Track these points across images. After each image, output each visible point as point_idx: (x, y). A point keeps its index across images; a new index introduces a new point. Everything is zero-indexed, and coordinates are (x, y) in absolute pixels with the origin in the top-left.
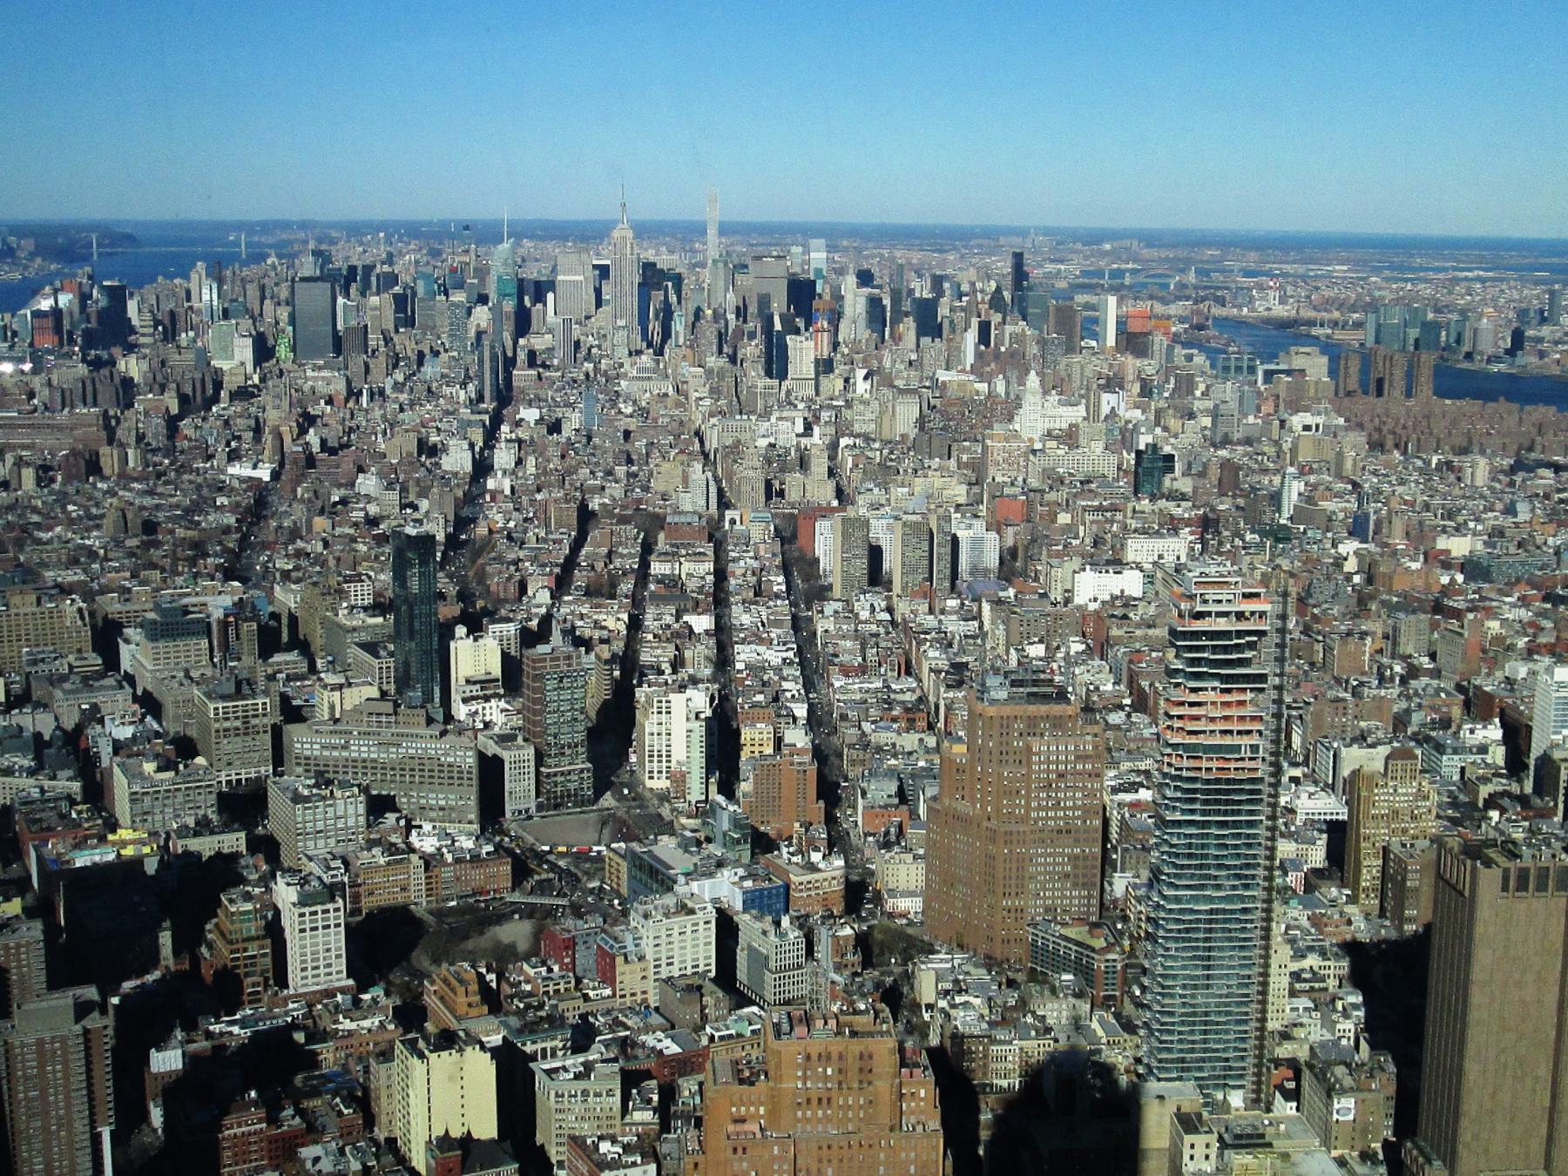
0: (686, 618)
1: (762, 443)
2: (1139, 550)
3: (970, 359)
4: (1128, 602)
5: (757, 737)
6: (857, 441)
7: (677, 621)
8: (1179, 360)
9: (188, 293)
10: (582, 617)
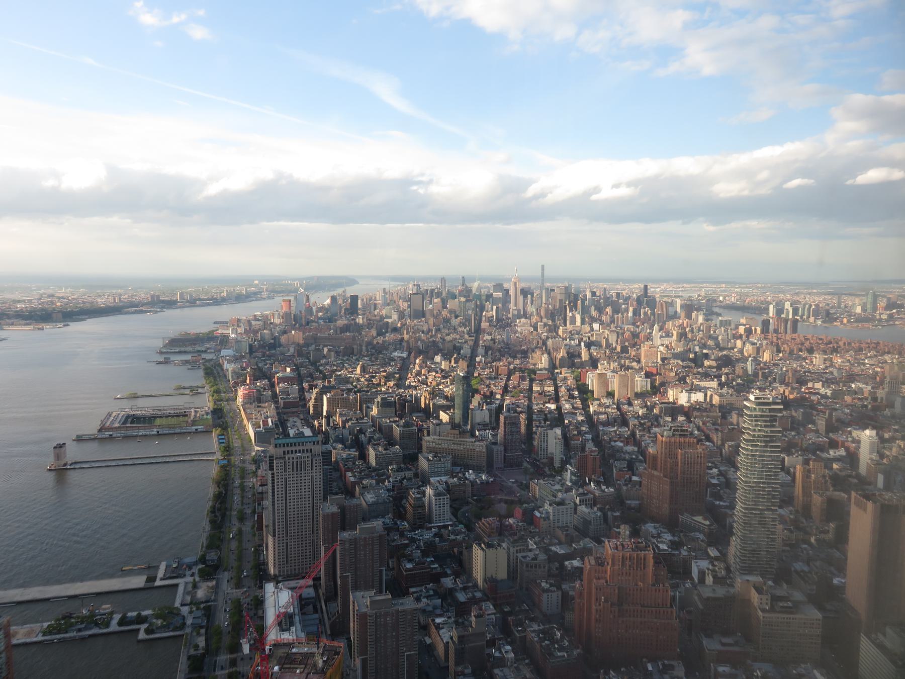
9: (375, 298)
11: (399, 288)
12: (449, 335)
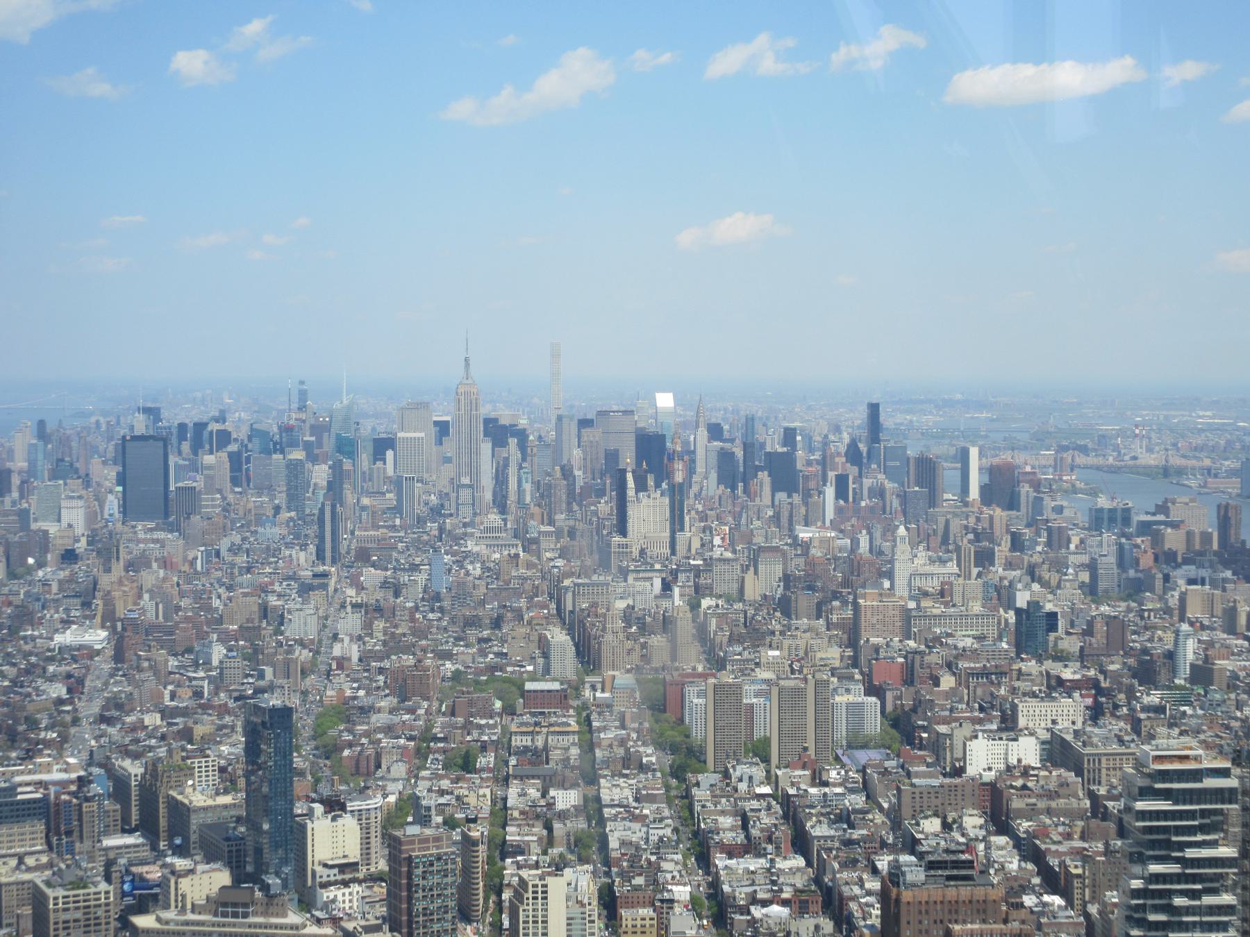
0: (552, 793)
1: (621, 605)
2: (1032, 714)
3: (830, 514)
4: (1026, 772)
5: (639, 923)
6: (720, 602)
7: (543, 796)
8: (1048, 514)
10: (442, 793)
11: (93, 419)
12: (249, 570)
